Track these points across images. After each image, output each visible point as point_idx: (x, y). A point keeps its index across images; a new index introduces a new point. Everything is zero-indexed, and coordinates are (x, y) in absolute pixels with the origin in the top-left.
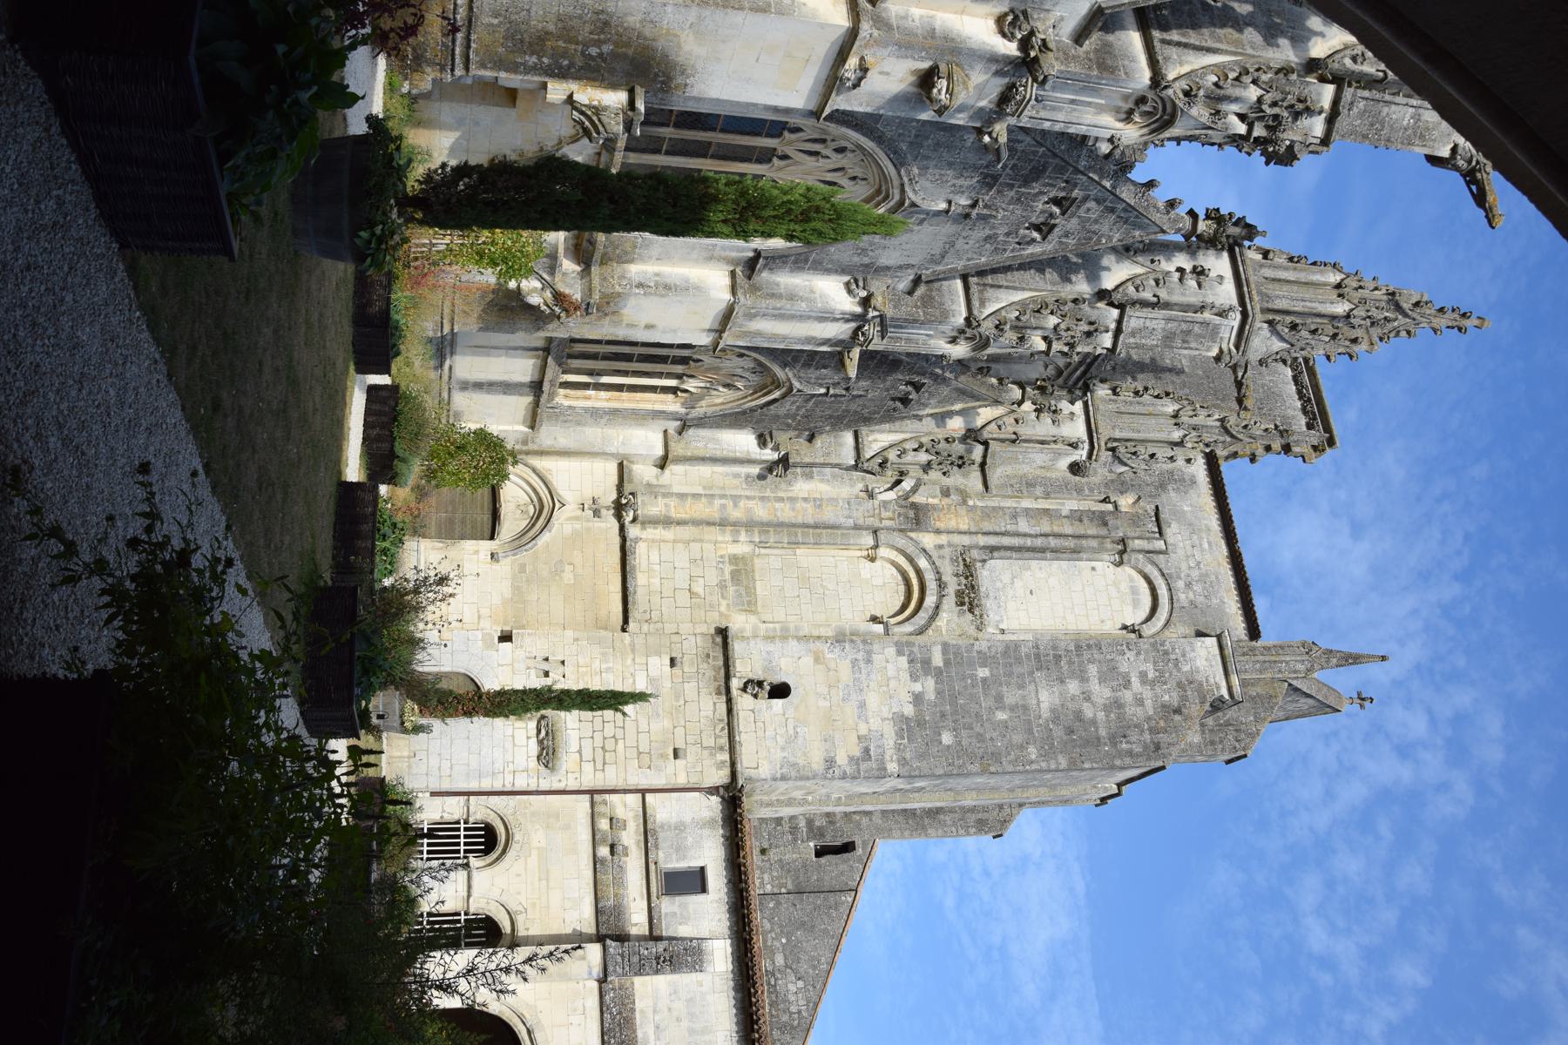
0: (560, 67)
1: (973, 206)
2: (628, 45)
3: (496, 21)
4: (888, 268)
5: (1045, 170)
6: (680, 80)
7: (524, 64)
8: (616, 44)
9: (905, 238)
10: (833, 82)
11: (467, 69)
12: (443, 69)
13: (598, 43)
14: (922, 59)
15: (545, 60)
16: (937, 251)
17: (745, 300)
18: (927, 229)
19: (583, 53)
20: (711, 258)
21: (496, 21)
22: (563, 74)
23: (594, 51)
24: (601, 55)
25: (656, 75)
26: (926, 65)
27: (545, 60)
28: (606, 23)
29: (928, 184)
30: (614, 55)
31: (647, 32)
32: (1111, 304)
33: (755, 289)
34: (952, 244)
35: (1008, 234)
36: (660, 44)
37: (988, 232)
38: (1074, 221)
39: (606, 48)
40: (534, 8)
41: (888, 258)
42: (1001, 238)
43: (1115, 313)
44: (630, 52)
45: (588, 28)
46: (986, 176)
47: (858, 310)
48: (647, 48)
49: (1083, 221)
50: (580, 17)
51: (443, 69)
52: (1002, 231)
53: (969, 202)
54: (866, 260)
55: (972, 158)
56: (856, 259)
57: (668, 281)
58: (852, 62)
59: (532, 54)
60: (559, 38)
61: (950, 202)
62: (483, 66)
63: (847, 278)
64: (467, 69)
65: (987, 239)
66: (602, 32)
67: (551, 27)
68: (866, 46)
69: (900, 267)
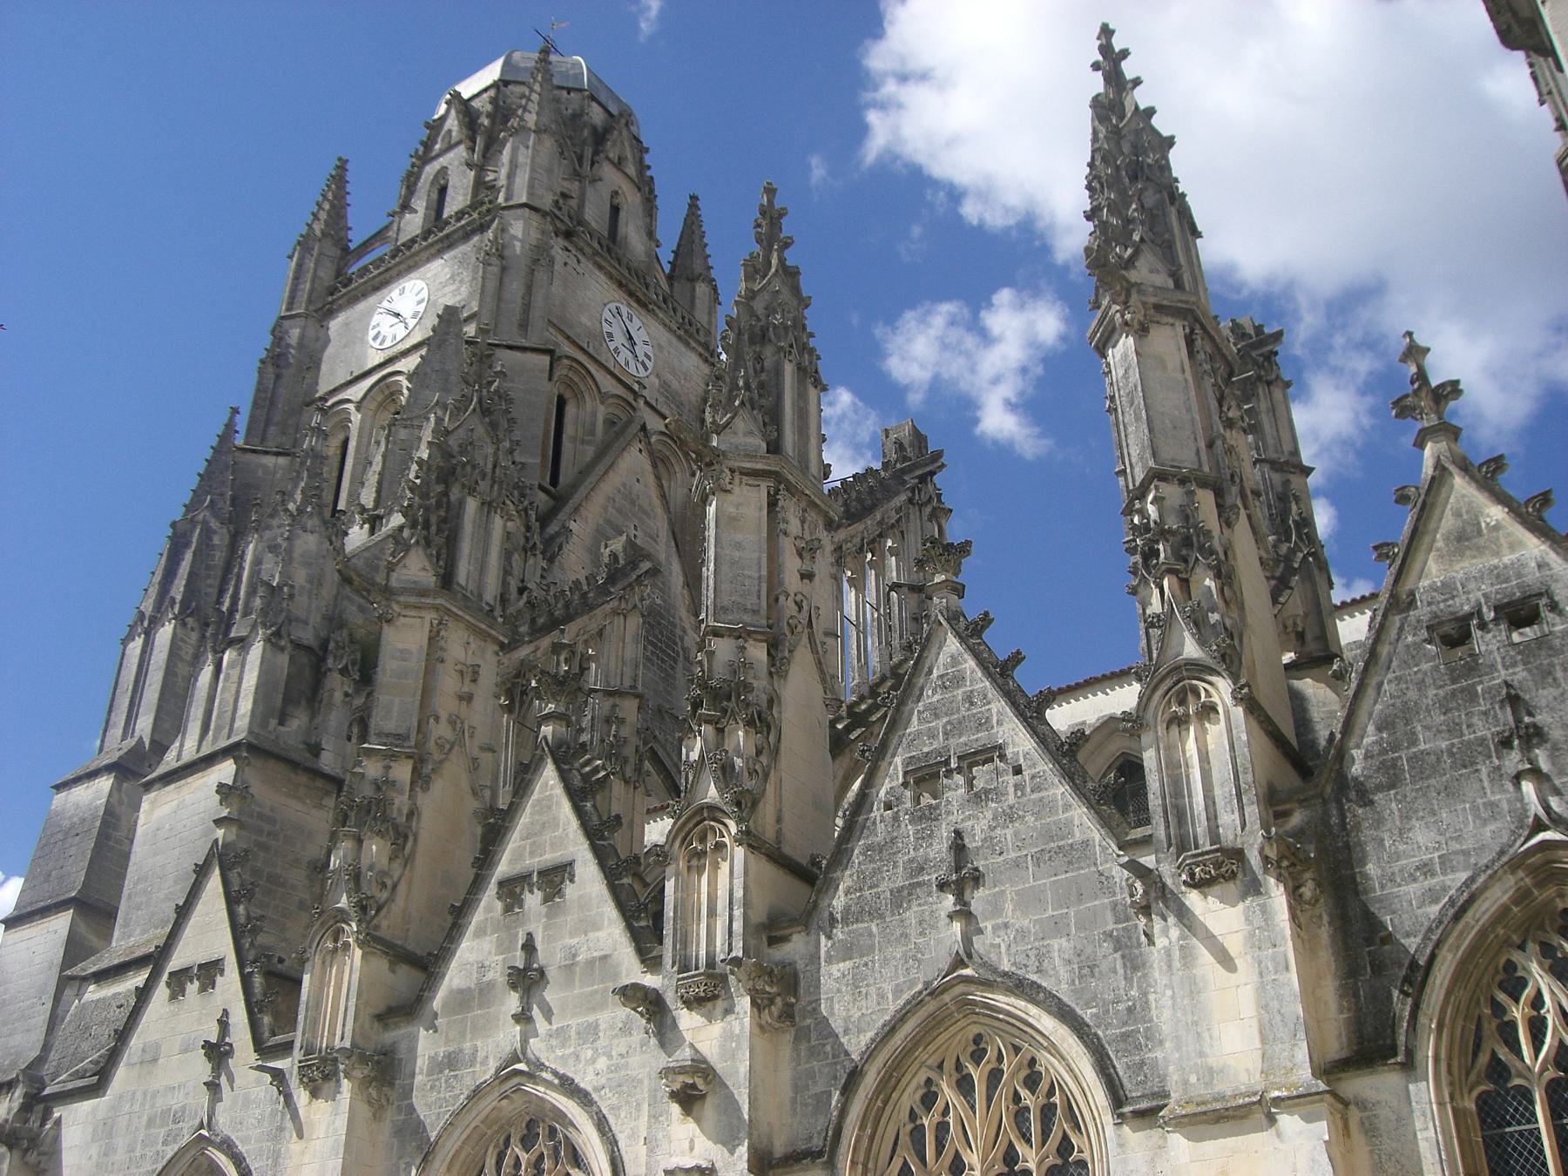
26: (675, 1109)
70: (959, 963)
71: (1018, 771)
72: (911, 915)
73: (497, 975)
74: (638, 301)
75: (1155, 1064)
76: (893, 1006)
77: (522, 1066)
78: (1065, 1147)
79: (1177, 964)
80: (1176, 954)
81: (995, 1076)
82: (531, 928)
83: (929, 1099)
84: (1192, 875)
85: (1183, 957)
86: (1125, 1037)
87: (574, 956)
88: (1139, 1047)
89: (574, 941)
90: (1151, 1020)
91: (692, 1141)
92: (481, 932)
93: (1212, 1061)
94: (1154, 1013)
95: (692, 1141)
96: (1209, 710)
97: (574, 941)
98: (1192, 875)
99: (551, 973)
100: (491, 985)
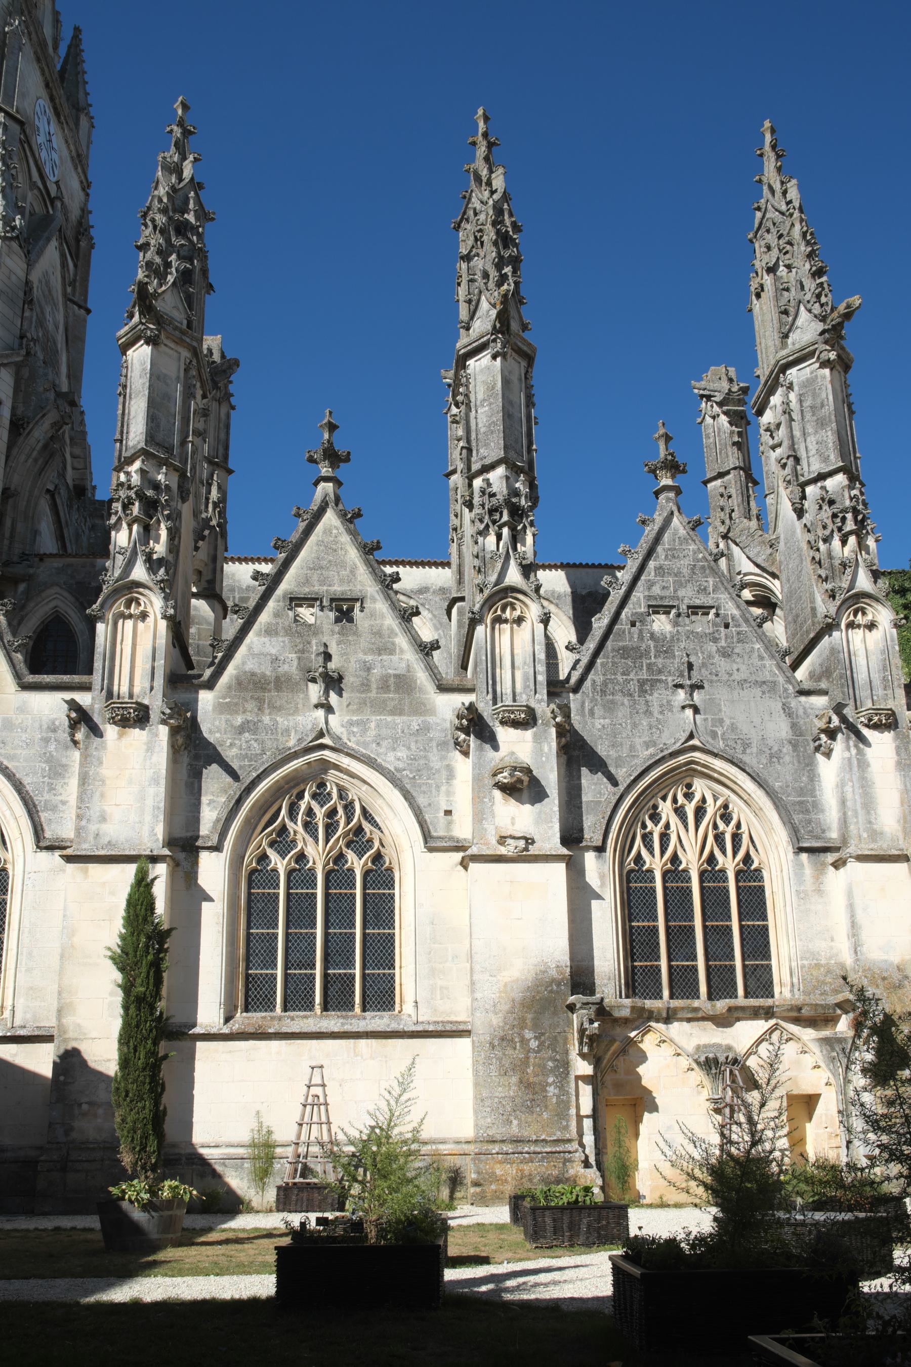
0: (557, 1067)
1: (681, 686)
2: (523, 1020)
3: (515, 1122)
4: (794, 726)
5: (624, 648)
6: (553, 973)
7: (558, 1097)
8: (522, 1028)
9: (745, 728)
10: (527, 854)
11: (569, 1141)
12: (570, 1160)
13: (524, 1041)
14: (492, 799)
15: (551, 1080)
16: (757, 691)
17: (853, 849)
18: (726, 712)
19: (537, 1052)
20: (819, 892)
21: (515, 1122)
22: (565, 1065)
23: (534, 1044)
24: (536, 1038)
25: (551, 991)
26: (497, 793)
27: (551, 1080)
28: (503, 1039)
29: (666, 734)
30: (536, 1026)
31: (506, 1007)
32: (804, 497)
33: (845, 840)
34: (742, 683)
35: (715, 640)
36: (518, 995)
37: (717, 659)
38: (681, 593)
39: (528, 1034)
40: (497, 1094)
41: (780, 729)
42: (723, 643)
43: (809, 490)
44: (529, 1016)
45: (509, 1051)
46: (642, 692)
47: (840, 736)
48: (523, 1005)
49: (679, 585)
50: (500, 1059)
51: (570, 1160)
52: (712, 647)
53: (680, 691)
54: (787, 749)
55: (622, 713)
56: (787, 759)
57: (850, 924)
58: (503, 850)
59: (546, 1091)
60: (523, 1072)
61: (683, 707)
62: (566, 1128)
63: (819, 757)
64: (569, 1141)
65: (725, 654)
66: (512, 1040)
67: (514, 1080)
68: (486, 844)
69: (790, 715)
70: (691, 736)
71: (727, 626)
72: (656, 698)
73: (291, 666)
74: (55, 109)
75: (819, 823)
76: (645, 755)
77: (326, 741)
78: (747, 859)
79: (855, 769)
80: (855, 762)
81: (700, 812)
82: (325, 639)
83: (655, 817)
84: (870, 720)
85: (859, 766)
86: (801, 803)
87: (369, 670)
88: (807, 811)
89: (369, 658)
90: (815, 797)
91: (513, 818)
92: (270, 631)
93: (875, 827)
94: (818, 793)
95: (513, 818)
96: (871, 626)
97: (369, 658)
98: (870, 720)
99: (349, 680)
100: (288, 678)
